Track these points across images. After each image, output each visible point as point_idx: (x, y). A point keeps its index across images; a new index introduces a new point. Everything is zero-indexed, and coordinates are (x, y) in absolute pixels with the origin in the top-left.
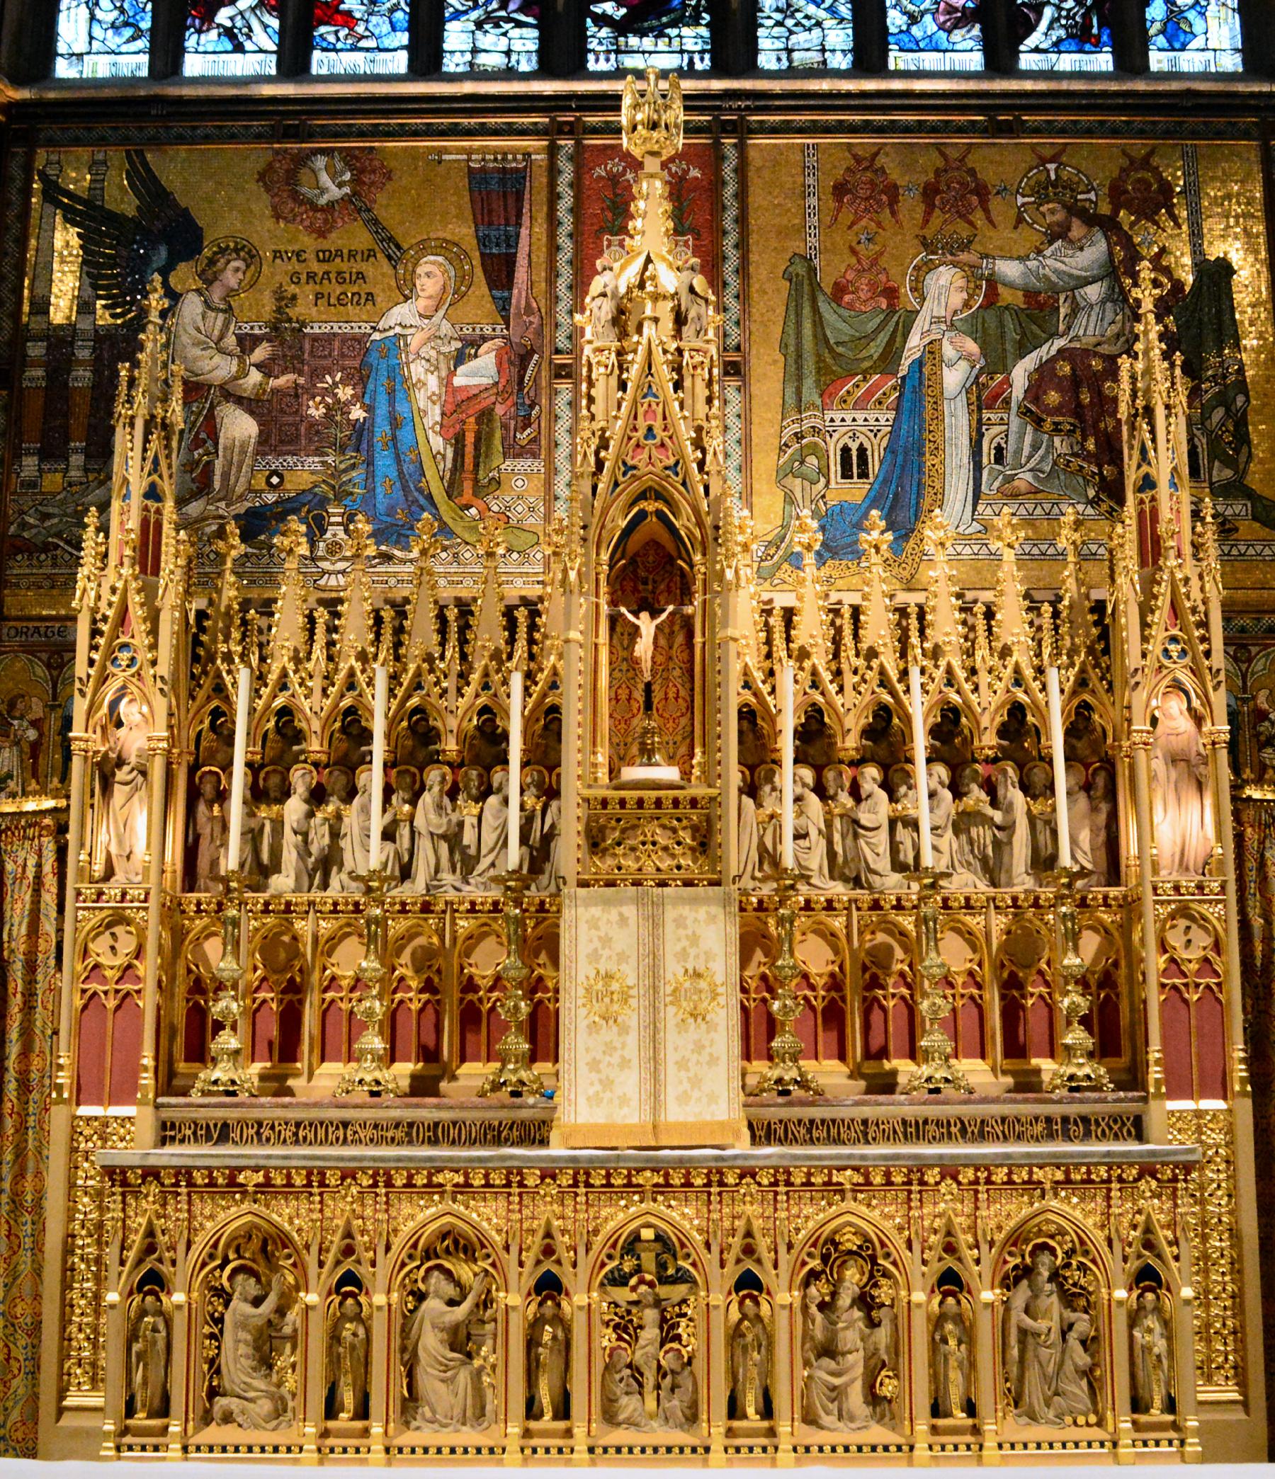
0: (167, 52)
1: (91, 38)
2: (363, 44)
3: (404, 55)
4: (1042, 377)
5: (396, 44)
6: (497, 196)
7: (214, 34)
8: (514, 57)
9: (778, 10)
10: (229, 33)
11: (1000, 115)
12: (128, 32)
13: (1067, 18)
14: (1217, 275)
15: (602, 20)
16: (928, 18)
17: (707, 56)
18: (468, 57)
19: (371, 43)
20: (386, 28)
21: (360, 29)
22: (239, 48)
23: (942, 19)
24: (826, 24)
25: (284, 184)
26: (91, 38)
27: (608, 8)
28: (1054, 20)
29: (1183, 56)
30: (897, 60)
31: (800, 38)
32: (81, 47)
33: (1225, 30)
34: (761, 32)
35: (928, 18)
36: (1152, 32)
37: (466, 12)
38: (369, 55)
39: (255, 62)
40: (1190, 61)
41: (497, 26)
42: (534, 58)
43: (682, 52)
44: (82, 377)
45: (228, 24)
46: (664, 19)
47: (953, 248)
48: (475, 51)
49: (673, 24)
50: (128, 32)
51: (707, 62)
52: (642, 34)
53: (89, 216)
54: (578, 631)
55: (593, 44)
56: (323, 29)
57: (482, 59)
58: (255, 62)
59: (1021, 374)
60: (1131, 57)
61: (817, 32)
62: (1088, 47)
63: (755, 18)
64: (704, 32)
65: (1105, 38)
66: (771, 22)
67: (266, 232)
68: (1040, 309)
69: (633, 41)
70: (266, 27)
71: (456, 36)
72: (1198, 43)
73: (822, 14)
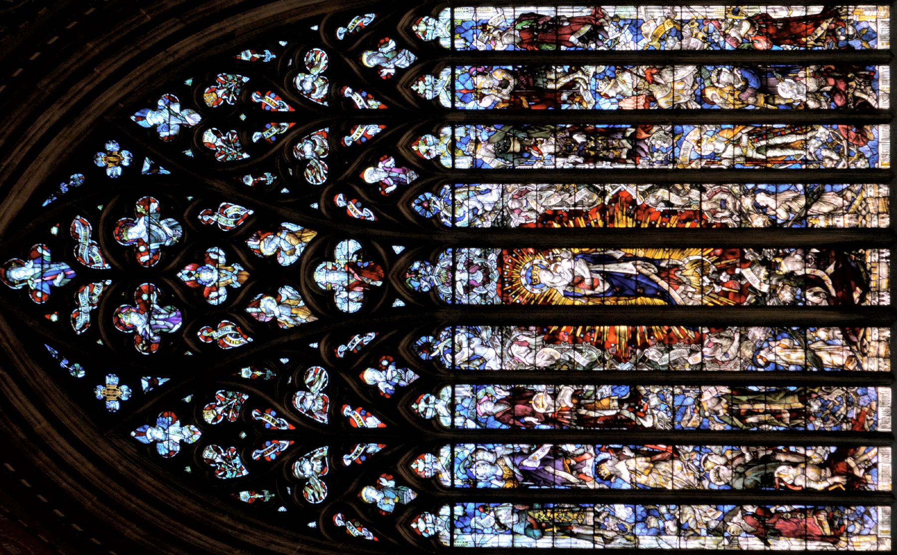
0: (879, 498)
1: (869, 534)
2: (874, 407)
3: (881, 390)
5: (874, 393)
7: (868, 477)
8: (881, 339)
9: (857, 218)
10: (867, 470)
12: (866, 517)
13: (860, 85)
15: (862, 298)
16: (861, 149)
17: (881, 251)
18: (881, 359)
19: (874, 404)
20: (866, 398)
21: (866, 409)
22: (875, 465)
23: (862, 143)
24: (864, 195)
26: (869, 534)
27: (856, 296)
28: (862, 91)
29: (880, 32)
30: (884, 163)
31: (871, 208)
32: (874, 540)
33: (867, 13)
34: (869, 226)
35: (861, 149)
36: (867, 47)
37: (858, 361)
38: (880, 405)
39: (883, 458)
40: (883, 30)
41: (865, 347)
42: (882, 329)
43: (879, 262)
45: (863, 471)
46: (862, 270)
48: (878, 356)
49: (864, 266)
50: (866, 517)
51: (884, 251)
52: (869, 280)
55: (875, 302)
56: (866, 426)
57: (882, 352)
58: (883, 458)
60: (879, 57)
61: (869, 201)
62: (875, 77)
63: (862, 228)
64: (869, 252)
65: (871, 69)
66: (864, 222)
69: (873, 284)
70: (865, 453)
71: (870, 366)
72: (873, 27)
73: (859, 198)
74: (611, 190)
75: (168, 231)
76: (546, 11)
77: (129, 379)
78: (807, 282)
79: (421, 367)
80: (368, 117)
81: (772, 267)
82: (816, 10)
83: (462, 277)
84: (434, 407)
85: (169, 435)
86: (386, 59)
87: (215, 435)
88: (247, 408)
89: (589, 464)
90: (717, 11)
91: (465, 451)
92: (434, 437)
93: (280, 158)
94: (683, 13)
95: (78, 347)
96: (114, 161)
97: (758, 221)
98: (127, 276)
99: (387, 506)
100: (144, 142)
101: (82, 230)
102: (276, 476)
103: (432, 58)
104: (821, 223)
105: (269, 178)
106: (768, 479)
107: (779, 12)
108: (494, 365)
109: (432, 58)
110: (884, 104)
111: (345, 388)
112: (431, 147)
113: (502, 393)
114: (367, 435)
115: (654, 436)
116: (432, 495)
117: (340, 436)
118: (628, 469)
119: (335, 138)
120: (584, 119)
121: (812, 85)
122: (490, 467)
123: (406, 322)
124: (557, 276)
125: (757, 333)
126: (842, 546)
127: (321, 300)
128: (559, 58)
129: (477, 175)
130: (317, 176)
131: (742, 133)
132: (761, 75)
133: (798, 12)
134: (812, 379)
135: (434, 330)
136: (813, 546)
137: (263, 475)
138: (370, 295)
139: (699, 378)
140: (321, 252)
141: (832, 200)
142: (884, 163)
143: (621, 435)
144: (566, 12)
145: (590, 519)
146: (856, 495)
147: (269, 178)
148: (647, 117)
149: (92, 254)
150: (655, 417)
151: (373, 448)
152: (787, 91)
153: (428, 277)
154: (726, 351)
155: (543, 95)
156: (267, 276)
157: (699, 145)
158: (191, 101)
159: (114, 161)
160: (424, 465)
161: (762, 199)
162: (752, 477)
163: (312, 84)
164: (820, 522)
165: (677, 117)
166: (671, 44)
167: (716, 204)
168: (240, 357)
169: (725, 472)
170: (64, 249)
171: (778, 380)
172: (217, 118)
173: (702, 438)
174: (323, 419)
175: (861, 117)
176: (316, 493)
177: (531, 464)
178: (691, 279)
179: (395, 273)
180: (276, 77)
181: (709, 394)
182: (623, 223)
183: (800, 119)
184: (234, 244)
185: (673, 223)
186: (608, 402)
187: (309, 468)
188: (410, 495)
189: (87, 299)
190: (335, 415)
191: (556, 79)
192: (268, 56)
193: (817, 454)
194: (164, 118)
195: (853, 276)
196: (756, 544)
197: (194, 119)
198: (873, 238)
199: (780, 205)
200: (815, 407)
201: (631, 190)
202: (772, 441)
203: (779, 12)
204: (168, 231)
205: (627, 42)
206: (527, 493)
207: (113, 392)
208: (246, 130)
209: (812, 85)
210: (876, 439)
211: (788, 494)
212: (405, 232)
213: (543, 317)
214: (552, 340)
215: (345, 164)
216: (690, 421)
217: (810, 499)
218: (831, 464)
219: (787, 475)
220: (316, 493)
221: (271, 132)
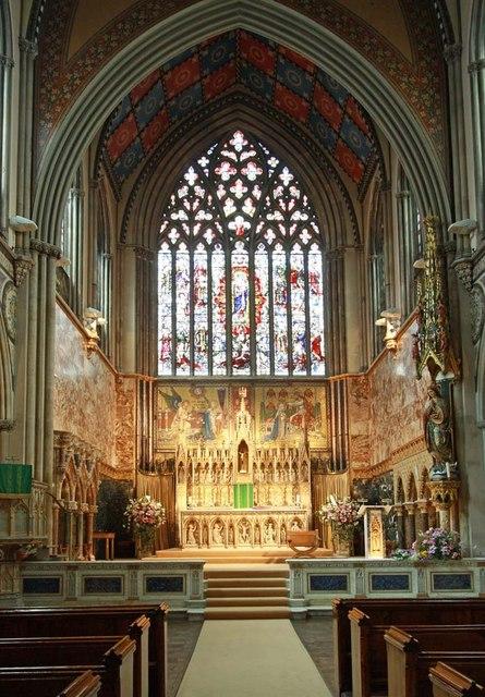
4: (294, 418)
6: (221, 394)
11: (289, 381)
14: (319, 405)
25: (192, 392)
30: (276, 374)
44: (166, 418)
47: (283, 402)
53: (166, 396)
54: (234, 453)
59: (291, 418)
67: (192, 399)
68: (294, 409)
71: (215, 370)
74: (267, 298)
75: (252, 177)
76: (320, 280)
77: (208, 166)
78: (240, 352)
79: (213, 245)
80: (288, 231)
81: (245, 342)
82: (323, 355)
83: (240, 255)
84: (200, 247)
85: (191, 176)
86: (305, 236)
87: (191, 190)
88: (200, 198)
89: (183, 291)
90: (322, 327)
91: (188, 257)
92: (191, 249)
93: (275, 206)
94: (321, 316)
95: (217, 152)
96: (273, 162)
97: (258, 338)
98: (239, 165)
99: (170, 236)
100: (279, 170)
101: (253, 153)
102: (179, 204)
103: (306, 249)
104: (258, 356)
105: (268, 204)
106: (179, 340)
107: (322, 344)
108: (213, 265)
109: (306, 249)
110: (294, 373)
111: (205, 224)
112: (279, 247)
113: (205, 267)
114: (191, 230)
115: (192, 309)
116: (174, 248)
117: (191, 223)
118: (182, 302)
119: (281, 222)
120: (288, 290)
121: (300, 353)
122: (183, 264)
123: (226, 241)
124: (240, 282)
125: (224, 338)
126: (160, 361)
127: (232, 218)
128: (307, 283)
129: (270, 261)
130: (270, 217)
131: (285, 334)
132: (302, 339)
133: (322, 349)
134: (210, 352)
135: (223, 249)
136: (159, 354)
137: (180, 203)
138: (234, 232)
139: (210, 321)
140: (247, 218)
141: (265, 359)
142: (276, 374)
143: (193, 298)
144: (321, 285)
145: (167, 291)
146: (176, 365)
147: (268, 204)
148: (288, 307)
149: (245, 156)
150: (198, 310)
151: (188, 232)
152: (298, 349)
153: (240, 246)
154: (219, 330)
155: (295, 281)
156: (239, 203)
157: (281, 323)
158: (292, 183)
159: (273, 162)
160: (183, 246)
161: (265, 340)
162: (180, 336)
163: (297, 216)
164: (166, 355)
165: (289, 316)
166: (311, 315)
167: (263, 328)
168: (215, 197)
169: (181, 329)
170: (246, 149)
171: (210, 344)
172: (286, 191)
173: (192, 322)
174: (196, 218)
175: (291, 366)
176: (174, 217)
177: (184, 275)
178: (240, 320)
179: (241, 238)
180: (299, 205)
181: (206, 325)
182: (257, 301)
183: (290, 350)
184: (249, 194)
185: (257, 315)
186: (202, 296)
187: (182, 215)
188: (174, 242)
189: (232, 156)
190: (197, 222)
191: (301, 282)
192: (305, 204)
193: (188, 355)
194: (286, 176)
195: (241, 364)
196: (160, 337)
197: (286, 183)
198: (254, 369)
199: (264, 345)
200: (202, 354)
201: (267, 303)
202: (192, 342)
203: (322, 344)
204: (252, 177)
205: (311, 302)
206: (174, 274)
207: (203, 162)
208: (283, 197)
209: (300, 353)
210: (193, 370)
211: (175, 346)
212: (252, 241)
213: (228, 279)
214: (221, 281)
215: (274, 225)
216: (196, 319)
217: (174, 352)
218: (184, 359)
219: (181, 346)
220: (174, 217)
221: (282, 204)
